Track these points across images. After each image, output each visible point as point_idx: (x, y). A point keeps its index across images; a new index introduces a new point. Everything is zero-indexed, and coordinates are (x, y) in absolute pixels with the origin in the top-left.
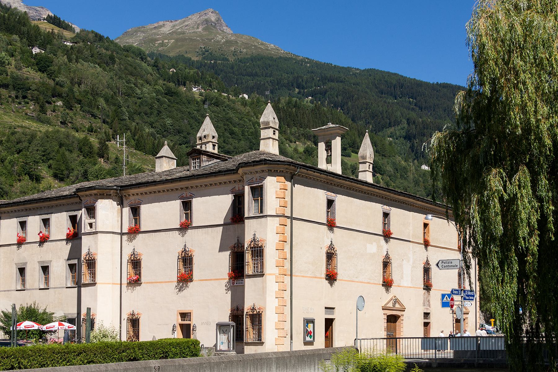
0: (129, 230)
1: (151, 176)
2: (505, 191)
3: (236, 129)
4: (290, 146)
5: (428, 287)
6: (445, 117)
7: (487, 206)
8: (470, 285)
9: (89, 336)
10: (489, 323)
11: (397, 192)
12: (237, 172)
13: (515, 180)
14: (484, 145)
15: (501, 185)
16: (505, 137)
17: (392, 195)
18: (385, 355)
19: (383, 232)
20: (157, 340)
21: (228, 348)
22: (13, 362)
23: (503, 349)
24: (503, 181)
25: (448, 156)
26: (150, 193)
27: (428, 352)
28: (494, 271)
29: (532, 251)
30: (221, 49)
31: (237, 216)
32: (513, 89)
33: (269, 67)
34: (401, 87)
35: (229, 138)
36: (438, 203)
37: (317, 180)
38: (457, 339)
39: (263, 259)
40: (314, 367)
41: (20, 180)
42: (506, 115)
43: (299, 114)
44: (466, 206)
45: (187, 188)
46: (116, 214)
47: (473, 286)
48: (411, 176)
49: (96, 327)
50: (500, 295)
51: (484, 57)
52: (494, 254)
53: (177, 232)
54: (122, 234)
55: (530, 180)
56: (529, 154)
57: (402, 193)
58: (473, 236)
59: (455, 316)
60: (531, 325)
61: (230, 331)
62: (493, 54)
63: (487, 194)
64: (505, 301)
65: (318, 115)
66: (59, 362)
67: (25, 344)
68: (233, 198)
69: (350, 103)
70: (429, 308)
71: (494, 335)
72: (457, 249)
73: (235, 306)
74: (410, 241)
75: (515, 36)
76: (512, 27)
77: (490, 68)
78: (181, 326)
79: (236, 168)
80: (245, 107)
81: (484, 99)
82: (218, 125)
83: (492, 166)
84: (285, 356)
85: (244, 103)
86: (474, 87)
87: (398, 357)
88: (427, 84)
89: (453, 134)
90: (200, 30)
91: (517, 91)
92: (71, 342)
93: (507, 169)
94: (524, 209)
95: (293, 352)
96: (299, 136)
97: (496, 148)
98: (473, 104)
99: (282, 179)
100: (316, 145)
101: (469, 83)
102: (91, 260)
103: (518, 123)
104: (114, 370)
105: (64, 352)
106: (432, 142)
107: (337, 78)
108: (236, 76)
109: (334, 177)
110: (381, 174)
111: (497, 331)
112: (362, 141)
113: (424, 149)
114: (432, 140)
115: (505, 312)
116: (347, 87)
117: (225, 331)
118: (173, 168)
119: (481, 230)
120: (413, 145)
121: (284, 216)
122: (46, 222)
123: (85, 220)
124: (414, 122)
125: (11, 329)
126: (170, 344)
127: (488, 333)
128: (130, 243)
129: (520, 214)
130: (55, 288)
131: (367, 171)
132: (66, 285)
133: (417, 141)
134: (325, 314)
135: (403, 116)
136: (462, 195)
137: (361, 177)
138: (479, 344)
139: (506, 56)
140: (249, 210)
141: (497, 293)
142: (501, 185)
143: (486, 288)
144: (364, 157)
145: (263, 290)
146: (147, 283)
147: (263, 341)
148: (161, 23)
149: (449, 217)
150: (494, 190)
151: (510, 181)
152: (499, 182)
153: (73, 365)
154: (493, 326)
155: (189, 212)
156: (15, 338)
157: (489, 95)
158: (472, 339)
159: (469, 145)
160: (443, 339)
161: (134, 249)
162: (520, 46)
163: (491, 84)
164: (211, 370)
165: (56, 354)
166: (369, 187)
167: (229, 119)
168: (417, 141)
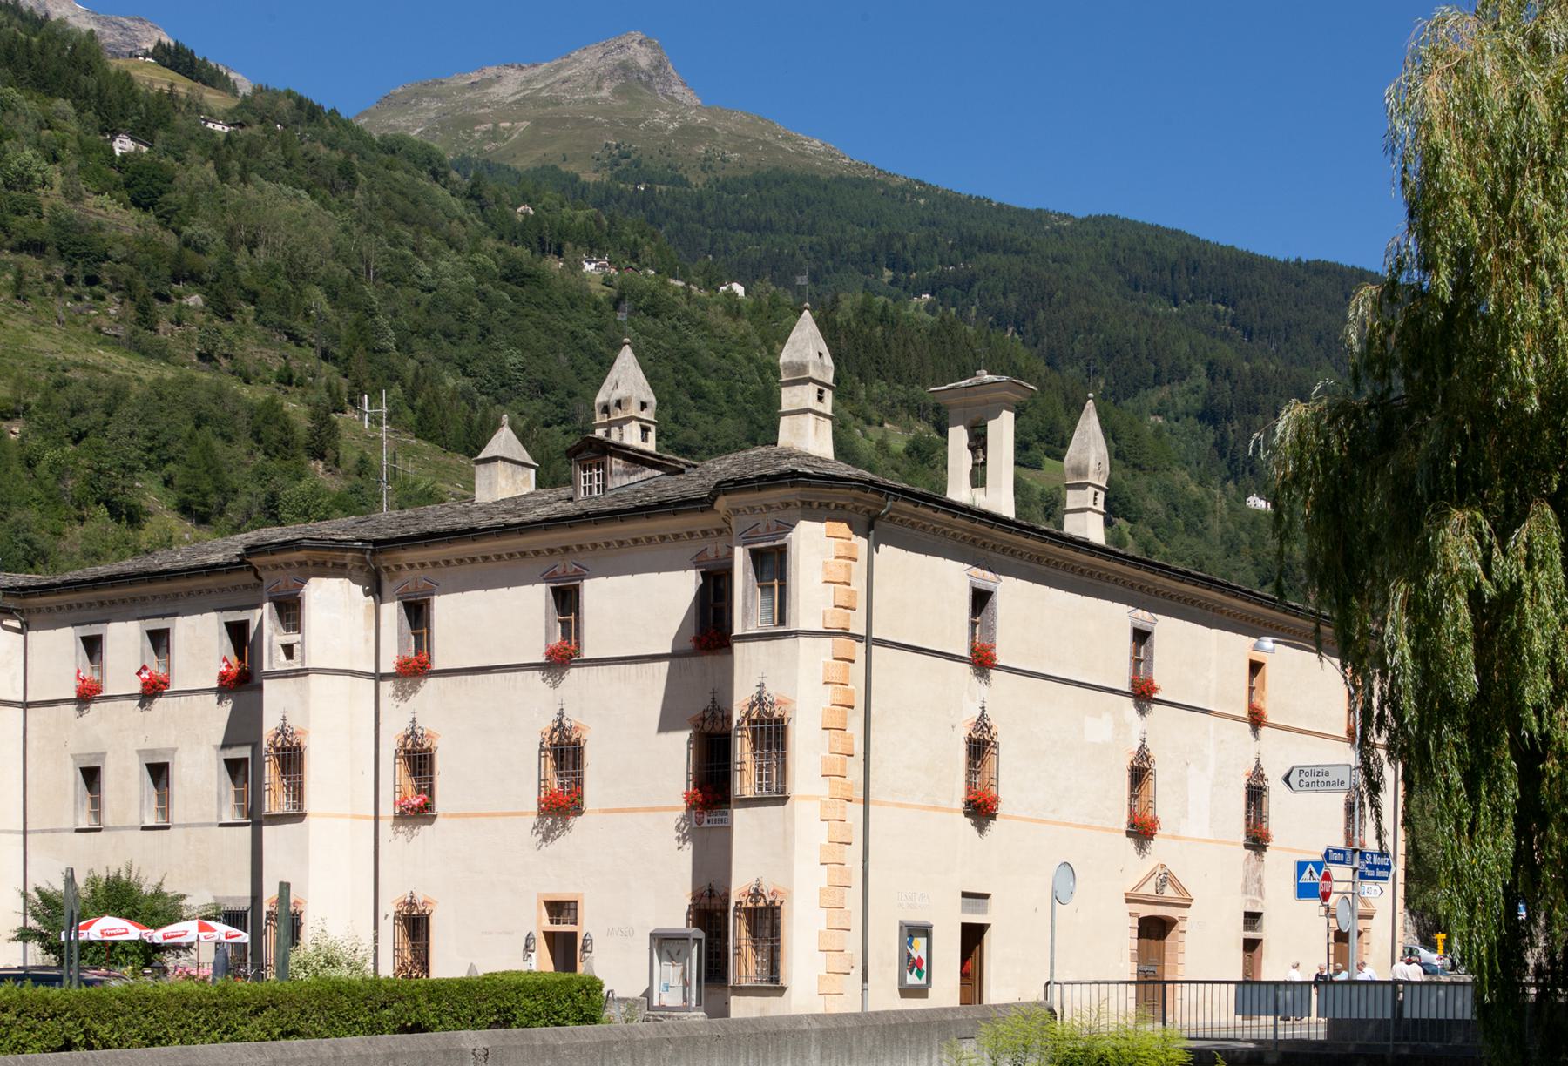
0: (400, 665)
1: (461, 512)
2: (1488, 573)
3: (709, 385)
4: (865, 435)
5: (1257, 841)
6: (1318, 359)
7: (1434, 617)
8: (1379, 837)
9: (285, 962)
10: (1429, 944)
11: (1175, 571)
12: (711, 508)
13: (1516, 543)
14: (1429, 440)
15: (1477, 555)
16: (1492, 420)
17: (1160, 580)
18: (1131, 1027)
19: (1133, 684)
20: (480, 974)
21: (685, 1000)
22: (69, 1029)
23: (1468, 1016)
24: (1481, 544)
25: (1326, 471)
26: (461, 561)
27: (1255, 1022)
28: (1448, 800)
29: (1561, 745)
30: (666, 152)
31: (712, 631)
32: (1518, 283)
33: (808, 206)
34: (1191, 271)
35: (687, 408)
36: (1294, 604)
37: (945, 532)
38: (1339, 987)
39: (784, 755)
40: (930, 1057)
41: (82, 520)
42: (1495, 355)
43: (892, 344)
44: (1373, 616)
45: (566, 549)
46: (360, 620)
47: (1389, 840)
48: (1217, 528)
49: (307, 935)
50: (1463, 868)
51: (1435, 189)
52: (1451, 753)
53: (538, 675)
54: (378, 677)
55: (1561, 544)
56: (1558, 470)
57: (1187, 574)
58: (1391, 699)
59: (1333, 922)
60: (1550, 951)
61: (689, 955)
62: (1463, 180)
63: (1436, 581)
64: (1479, 884)
65: (948, 346)
66: (202, 1032)
67: (102, 981)
68: (701, 581)
69: (1041, 315)
70: (1258, 899)
71: (1443, 979)
72: (1344, 735)
73: (704, 884)
74: (1208, 712)
75: (1529, 127)
76: (1521, 102)
77: (1455, 220)
78: (551, 937)
79: (710, 494)
80: (734, 320)
81: (1434, 308)
82: (656, 372)
83: (1451, 501)
84: (847, 1025)
85: (733, 308)
86: (1405, 273)
87: (1168, 1034)
88: (1268, 264)
89: (1340, 409)
90: (605, 93)
91: (1530, 286)
92: (235, 976)
93: (1495, 511)
94: (1540, 625)
95: (868, 1014)
96: (893, 406)
97: (1465, 450)
98: (1400, 323)
99: (843, 528)
100: (943, 432)
101: (1391, 262)
102: (289, 750)
103: (1531, 380)
104: (359, 1055)
105: (215, 1004)
106: (1279, 431)
107: (1005, 241)
108: (709, 231)
109: (992, 526)
110: (1128, 520)
111: (1454, 967)
112: (1074, 425)
113: (1256, 451)
114: (1280, 424)
115: (1478, 914)
116: (1033, 268)
117: (674, 955)
118: (526, 491)
119: (1415, 683)
120: (1223, 437)
121: (846, 634)
122: (159, 640)
123: (273, 635)
124: (1227, 371)
125: (63, 939)
126: (518, 988)
127: (1425, 972)
128: (402, 704)
129: (1529, 641)
130: (186, 826)
131: (1090, 509)
132: (220, 817)
133: (1237, 426)
134: (963, 911)
135: (1195, 354)
136: (1363, 583)
137: (1074, 526)
138: (1402, 1003)
139: (1502, 186)
140: (745, 615)
141: (1455, 861)
142: (1477, 555)
143: (1423, 846)
144: (1080, 471)
145: (785, 843)
146: (452, 816)
147: (783, 982)
148: (491, 72)
149: (1324, 645)
150: (1455, 569)
151: (1503, 545)
152: (1471, 547)
153: (242, 1040)
154: (1440, 951)
155: (572, 617)
156: (75, 962)
157: (1449, 298)
158: (1380, 987)
159: (1388, 440)
160: (1299, 987)
161: (414, 721)
162: (1542, 156)
163: (1456, 265)
164: (634, 1061)
165: (193, 1010)
166: (1093, 555)
167: (689, 355)
168: (1237, 426)
